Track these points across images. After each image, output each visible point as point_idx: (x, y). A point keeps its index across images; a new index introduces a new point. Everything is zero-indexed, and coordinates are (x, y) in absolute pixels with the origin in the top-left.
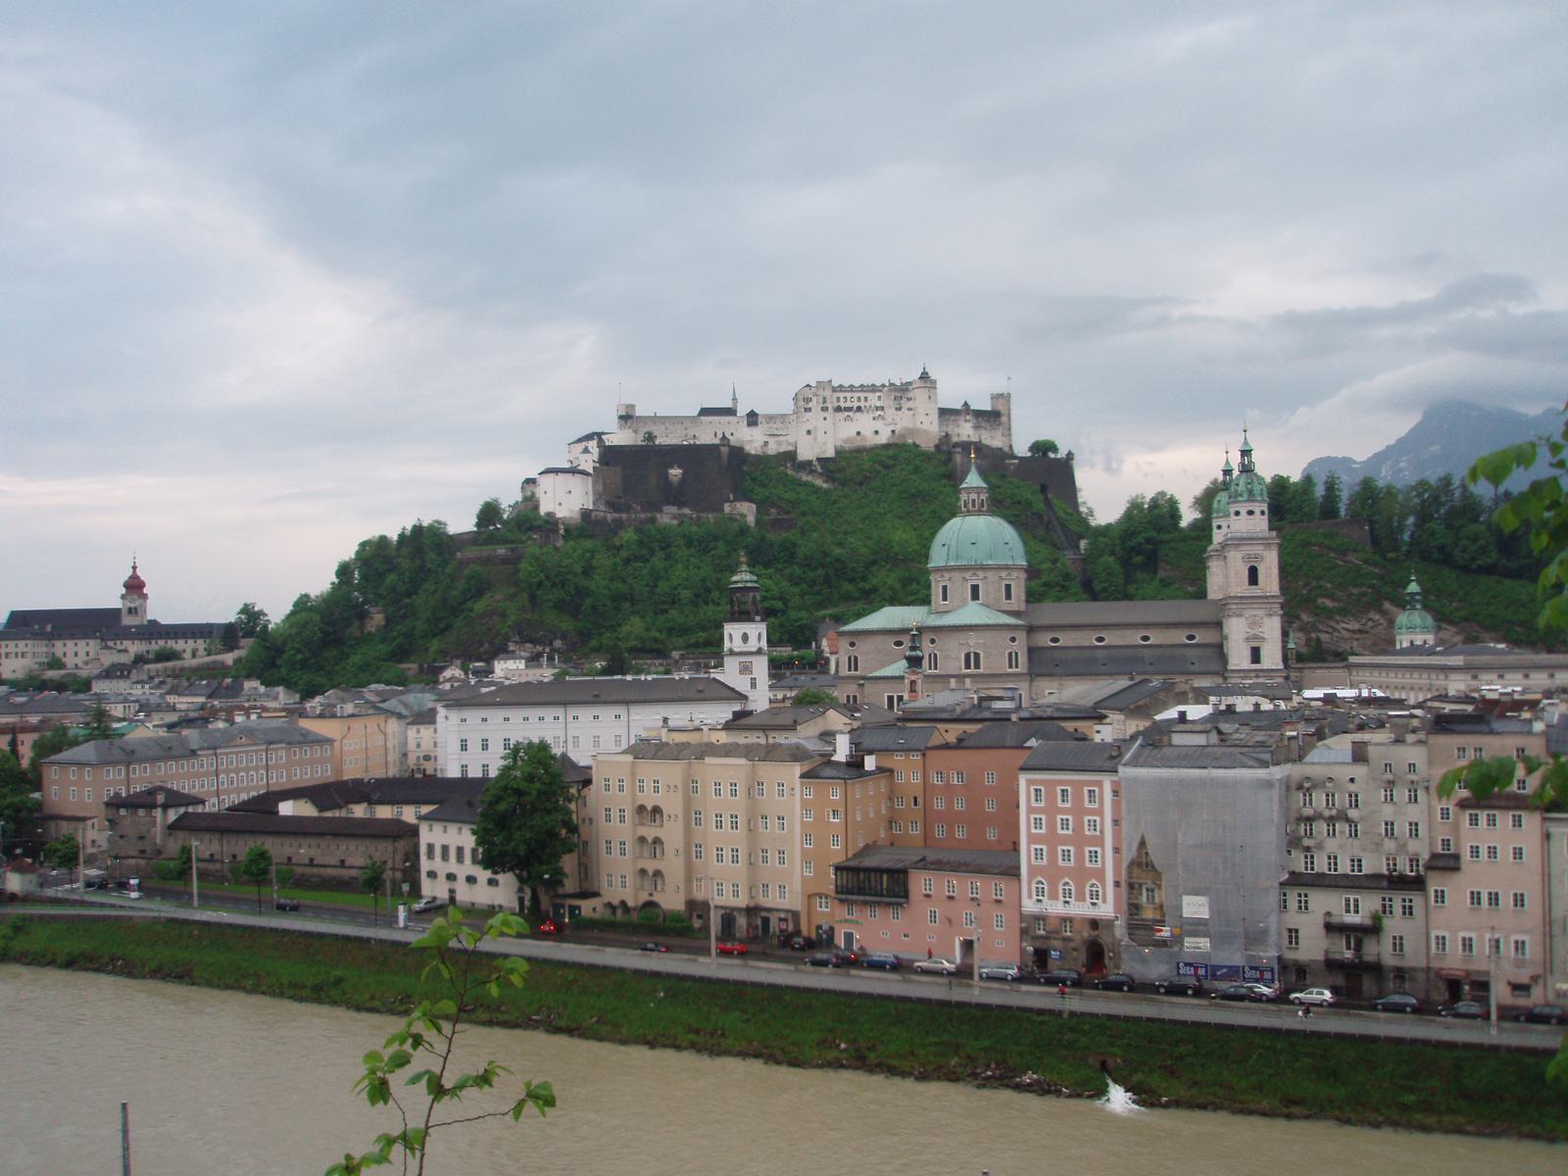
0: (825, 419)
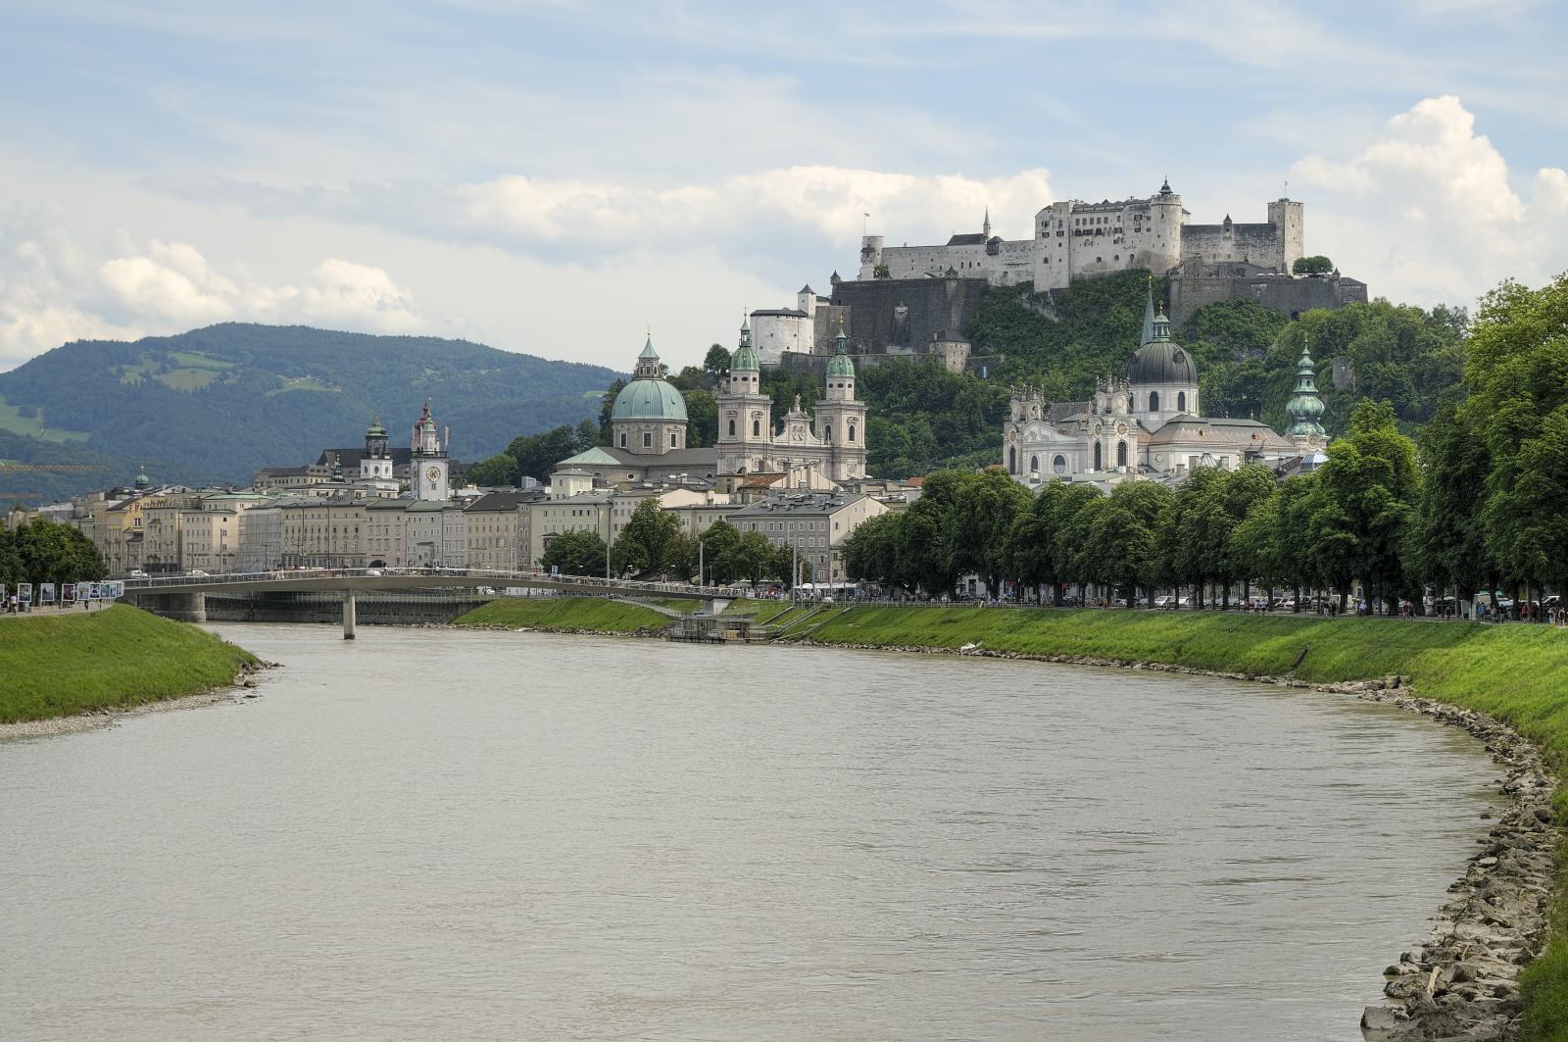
0: (1060, 245)
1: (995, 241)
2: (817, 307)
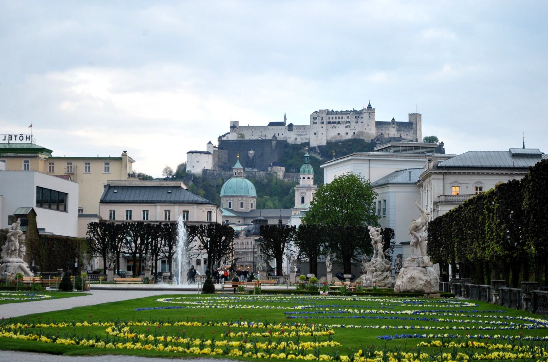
0: (322, 127)
1: (291, 125)
2: (214, 150)
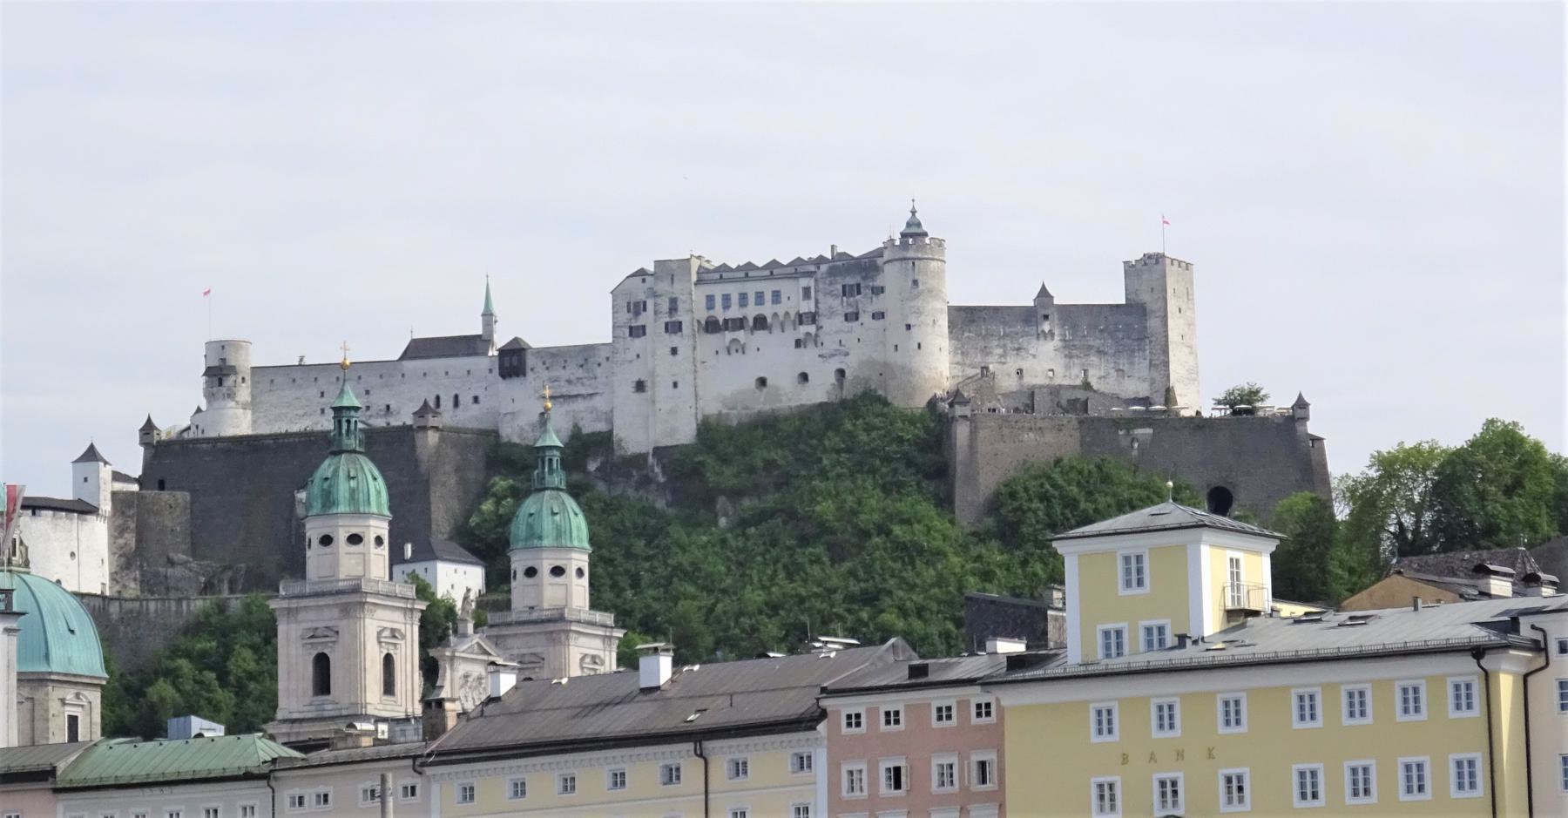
0: (674, 351)
2: (114, 494)
